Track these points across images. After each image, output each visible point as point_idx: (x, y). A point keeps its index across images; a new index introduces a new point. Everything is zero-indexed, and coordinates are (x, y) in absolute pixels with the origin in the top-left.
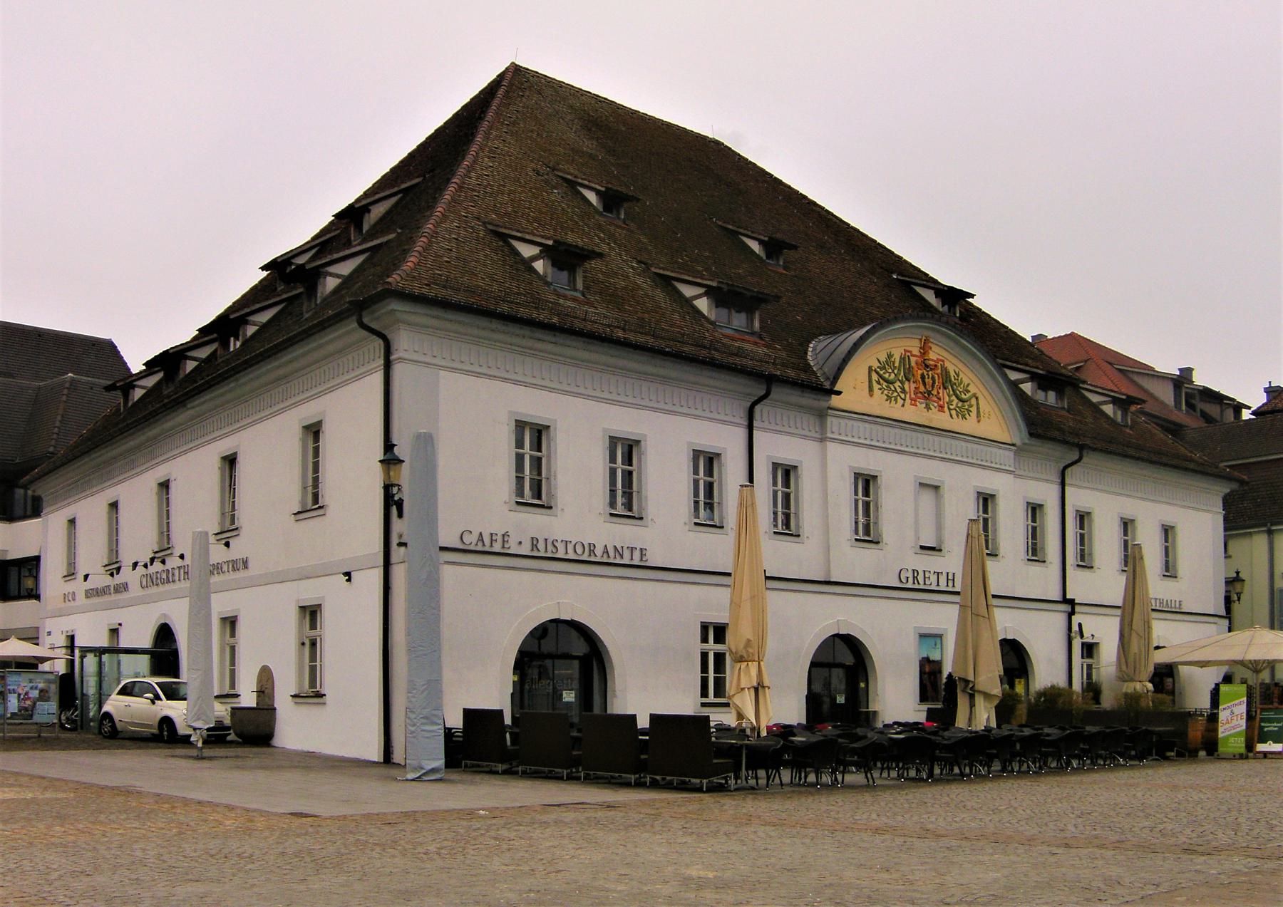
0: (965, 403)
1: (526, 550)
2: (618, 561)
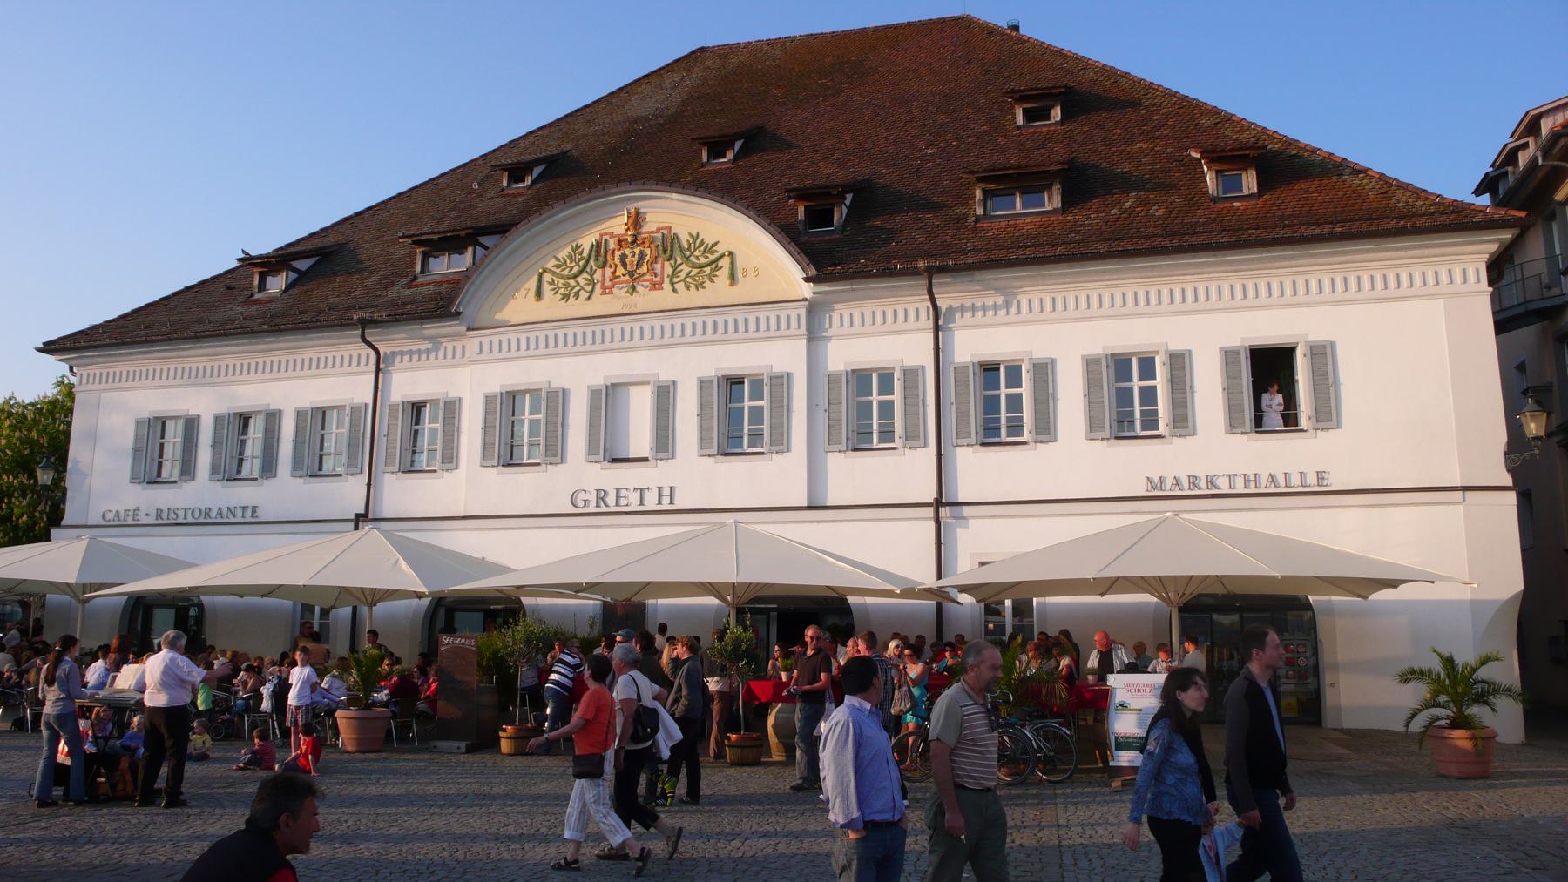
1: (152, 520)
2: (232, 520)
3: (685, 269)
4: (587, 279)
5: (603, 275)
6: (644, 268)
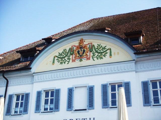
0: (103, 53)
3: (97, 54)
4: (67, 58)
5: (73, 57)
6: (85, 54)
